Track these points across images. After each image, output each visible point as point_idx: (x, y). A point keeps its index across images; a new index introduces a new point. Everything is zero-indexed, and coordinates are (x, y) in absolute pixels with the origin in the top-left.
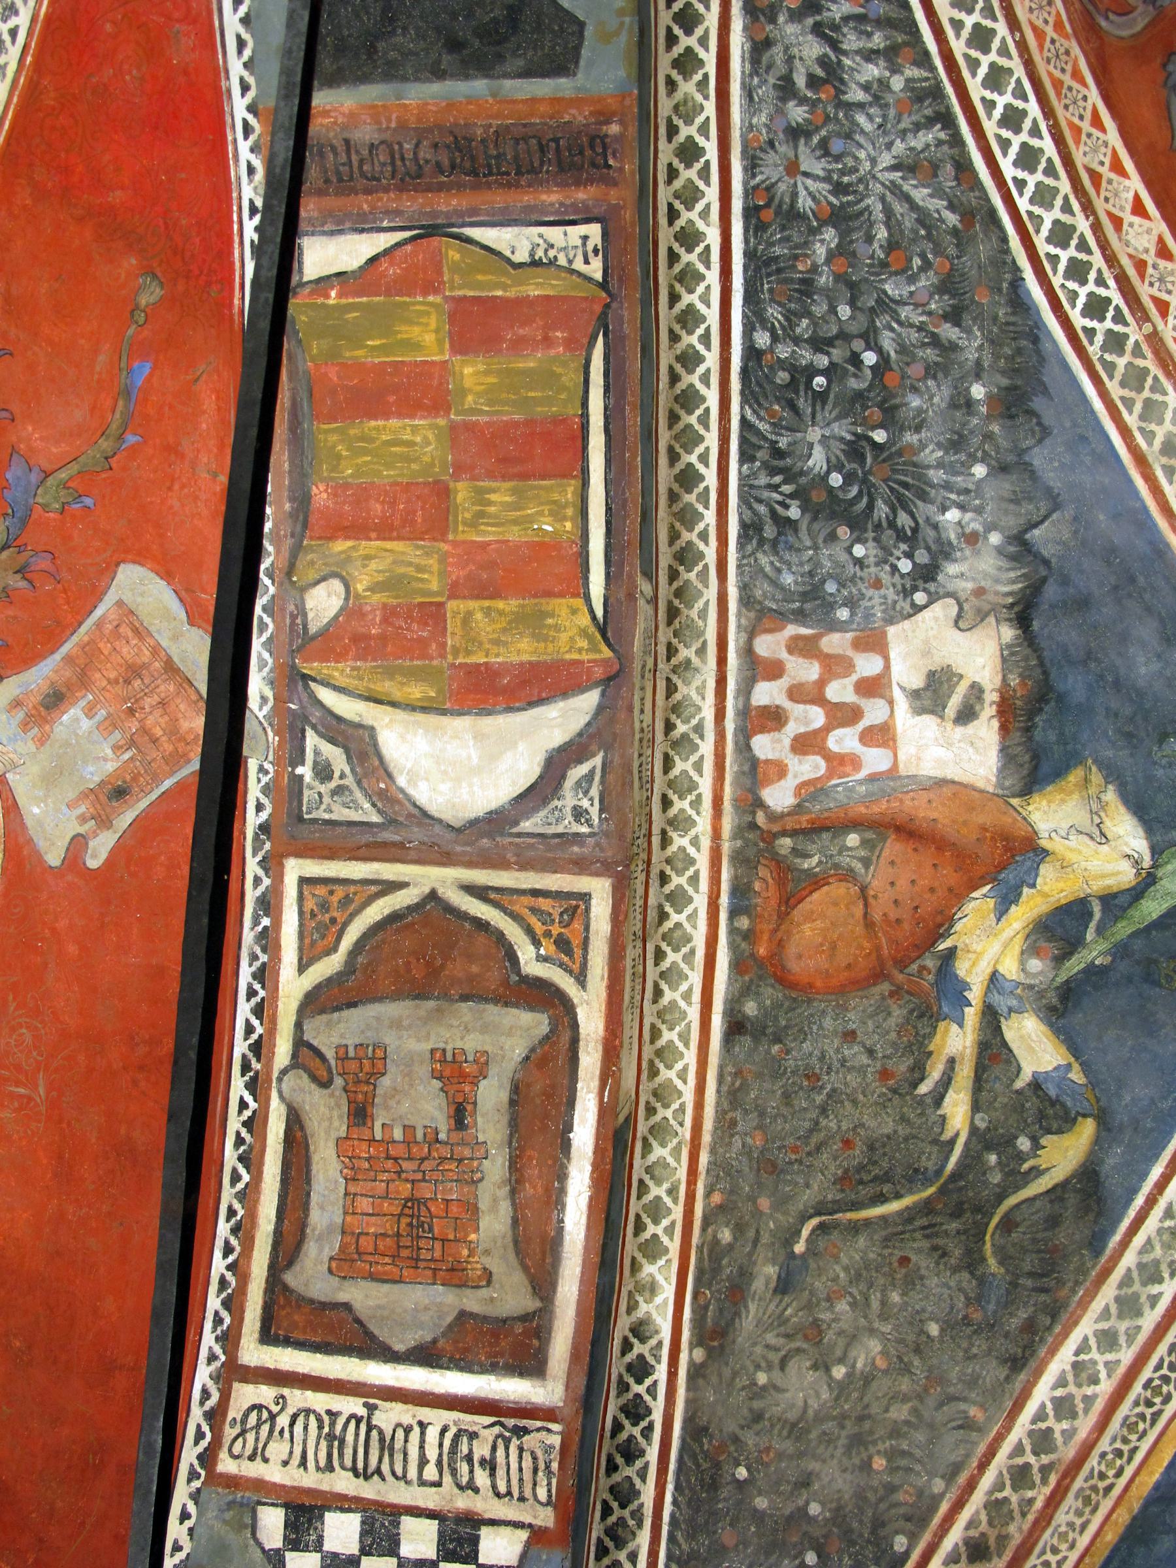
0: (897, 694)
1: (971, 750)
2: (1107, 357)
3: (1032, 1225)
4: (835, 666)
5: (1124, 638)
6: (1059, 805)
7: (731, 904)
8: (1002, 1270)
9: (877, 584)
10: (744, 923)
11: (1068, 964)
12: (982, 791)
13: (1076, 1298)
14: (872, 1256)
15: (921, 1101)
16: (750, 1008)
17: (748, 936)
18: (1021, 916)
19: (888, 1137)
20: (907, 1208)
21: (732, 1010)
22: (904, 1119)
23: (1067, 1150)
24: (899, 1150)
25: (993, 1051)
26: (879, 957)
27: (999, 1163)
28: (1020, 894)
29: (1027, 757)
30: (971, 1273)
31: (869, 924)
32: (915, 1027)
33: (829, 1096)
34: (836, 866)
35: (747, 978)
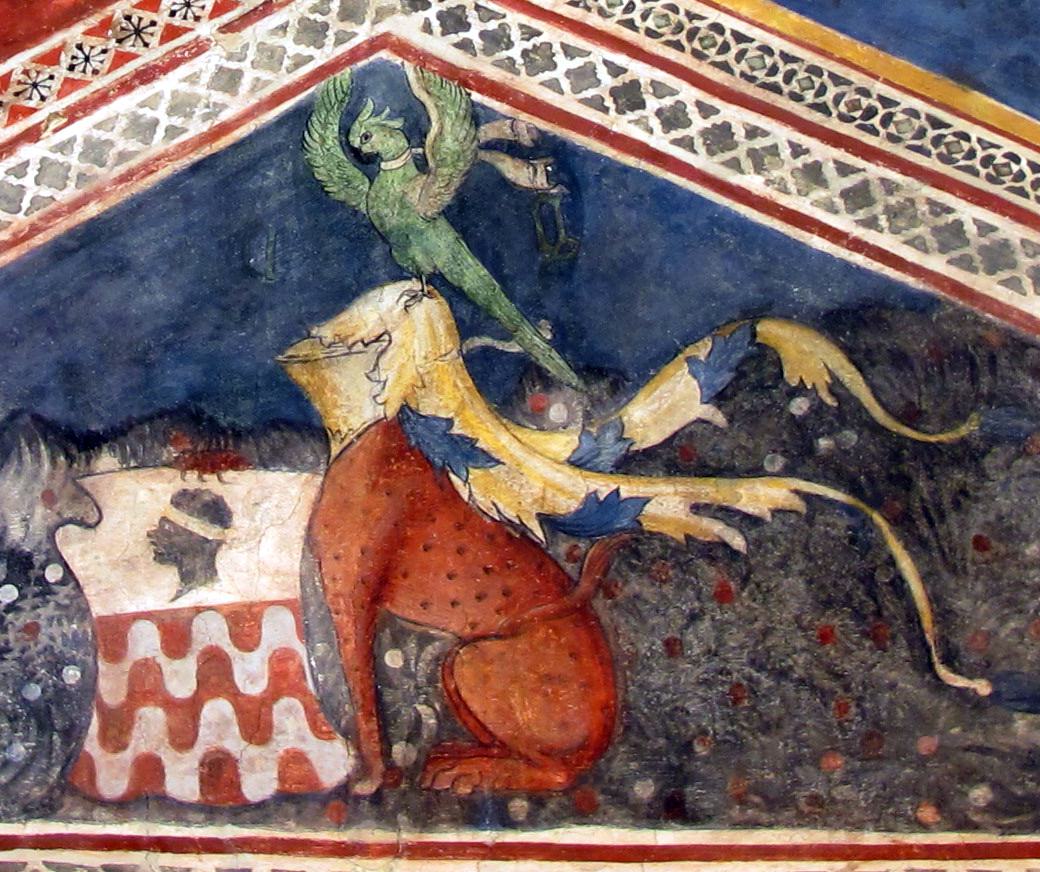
0: (186, 602)
1: (266, 505)
3: (908, 384)
4: (145, 686)
5: (118, 320)
6: (339, 393)
7: (493, 826)
8: (974, 415)
9: (32, 629)
10: (519, 806)
11: (553, 372)
12: (322, 491)
13: (997, 321)
14: (979, 588)
15: (756, 544)
16: (644, 790)
17: (538, 800)
18: (491, 434)
19: (810, 582)
20: (906, 547)
21: (649, 816)
22: (783, 564)
23: (802, 352)
24: (826, 567)
25: (678, 456)
26: (558, 615)
27: (829, 434)
28: (462, 438)
29: (275, 435)
30: (984, 454)
31: (512, 632)
32: (653, 561)
33: (761, 668)
34: (431, 681)
35: (601, 798)
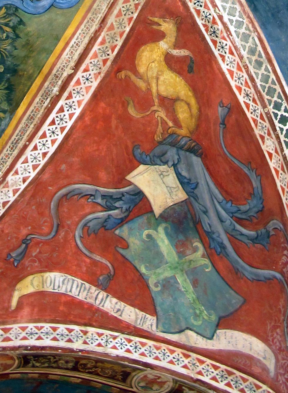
2: (280, 101)
